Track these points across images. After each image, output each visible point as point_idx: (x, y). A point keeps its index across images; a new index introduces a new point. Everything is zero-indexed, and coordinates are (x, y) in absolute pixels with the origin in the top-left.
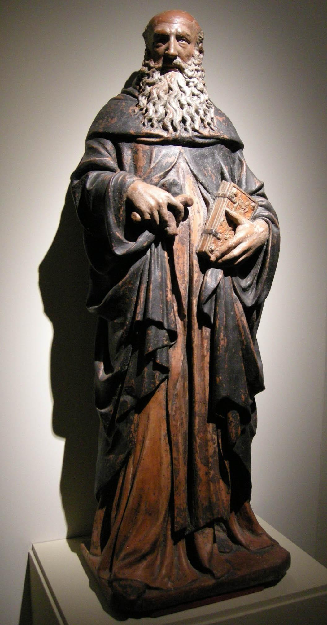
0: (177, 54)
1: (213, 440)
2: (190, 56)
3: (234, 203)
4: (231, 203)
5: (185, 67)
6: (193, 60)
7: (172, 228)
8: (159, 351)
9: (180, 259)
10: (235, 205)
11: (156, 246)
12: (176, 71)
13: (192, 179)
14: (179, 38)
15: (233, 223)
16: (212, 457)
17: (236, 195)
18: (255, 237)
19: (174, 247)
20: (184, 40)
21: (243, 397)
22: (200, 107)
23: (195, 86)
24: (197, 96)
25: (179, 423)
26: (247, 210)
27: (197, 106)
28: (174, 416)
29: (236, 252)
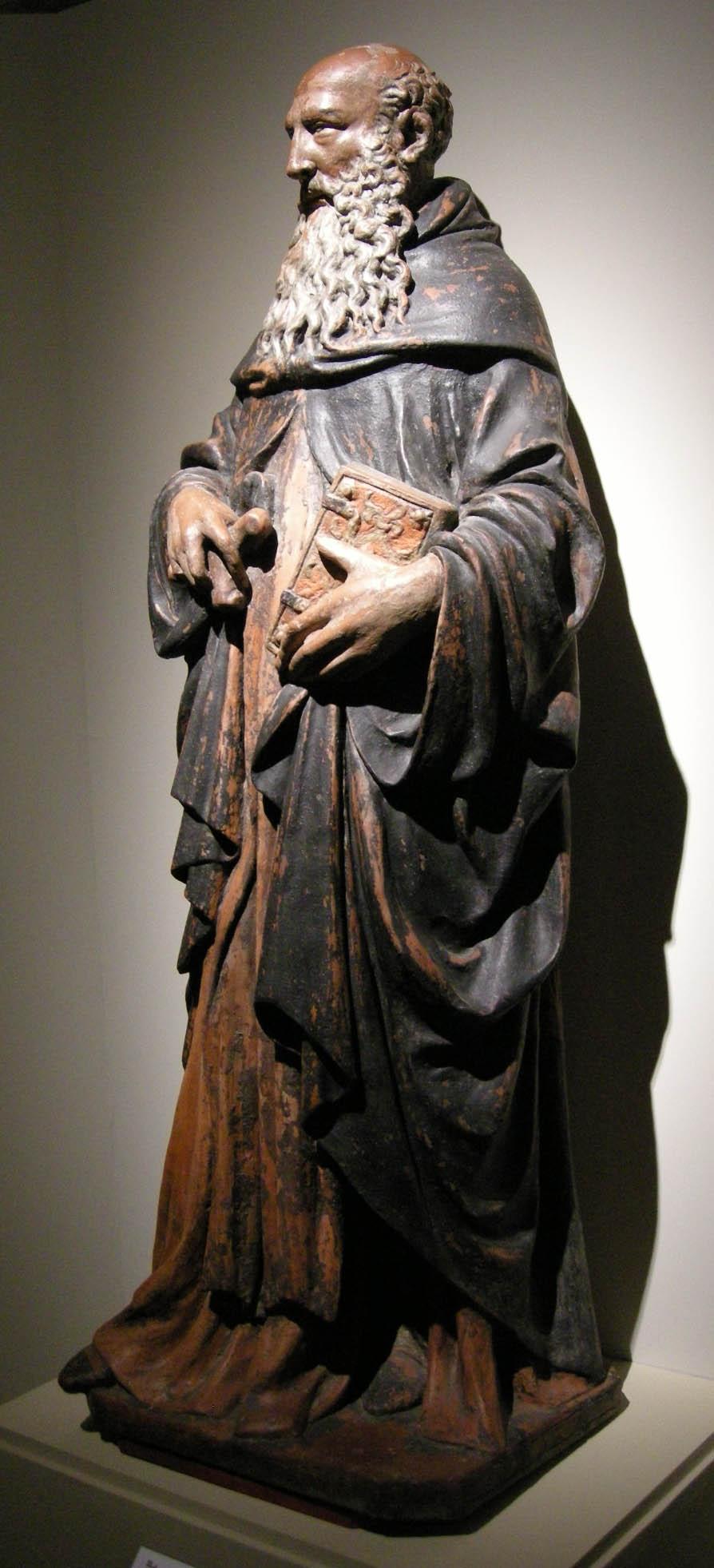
0: (306, 164)
1: (282, 1105)
2: (348, 157)
3: (348, 518)
4: (337, 517)
5: (332, 192)
6: (357, 165)
7: (225, 591)
8: (193, 869)
9: (254, 662)
10: (352, 523)
11: (217, 633)
12: (323, 205)
13: (310, 465)
14: (313, 124)
15: (337, 570)
16: (282, 1147)
17: (350, 497)
18: (365, 604)
19: (245, 634)
20: (323, 127)
21: (314, 1011)
22: (352, 281)
23: (352, 231)
24: (352, 253)
25: (223, 1044)
26: (397, 530)
27: (346, 282)
28: (216, 1025)
29: (312, 642)
